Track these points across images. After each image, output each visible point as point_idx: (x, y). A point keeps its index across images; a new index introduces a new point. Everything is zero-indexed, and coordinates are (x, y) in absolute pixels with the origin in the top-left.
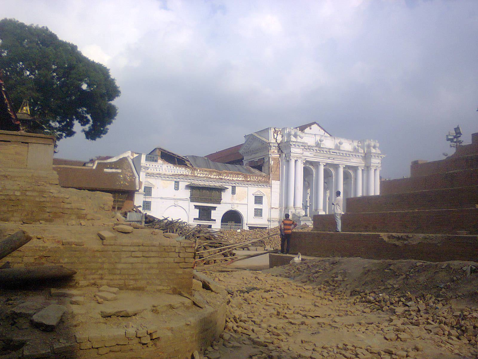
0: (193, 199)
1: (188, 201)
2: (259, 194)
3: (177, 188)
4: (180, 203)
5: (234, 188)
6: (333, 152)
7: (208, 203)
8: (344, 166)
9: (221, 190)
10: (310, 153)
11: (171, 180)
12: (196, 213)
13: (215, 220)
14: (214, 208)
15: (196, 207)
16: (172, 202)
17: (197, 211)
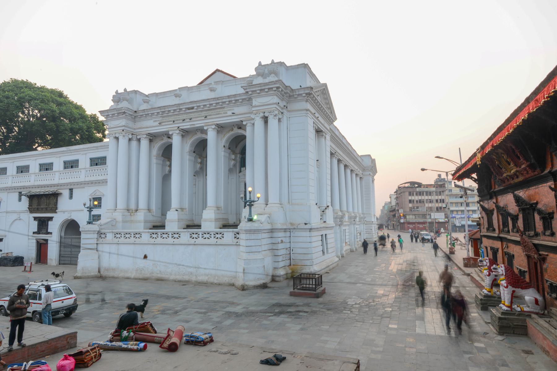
0: (31, 210)
1: (27, 214)
2: (97, 195)
3: (20, 200)
4: (23, 216)
5: (71, 190)
6: (189, 109)
7: (45, 213)
8: (214, 127)
9: (56, 195)
10: (155, 121)
11: (14, 192)
12: (34, 226)
13: (51, 233)
14: (51, 219)
15: (35, 218)
16: (15, 216)
17: (36, 223)
